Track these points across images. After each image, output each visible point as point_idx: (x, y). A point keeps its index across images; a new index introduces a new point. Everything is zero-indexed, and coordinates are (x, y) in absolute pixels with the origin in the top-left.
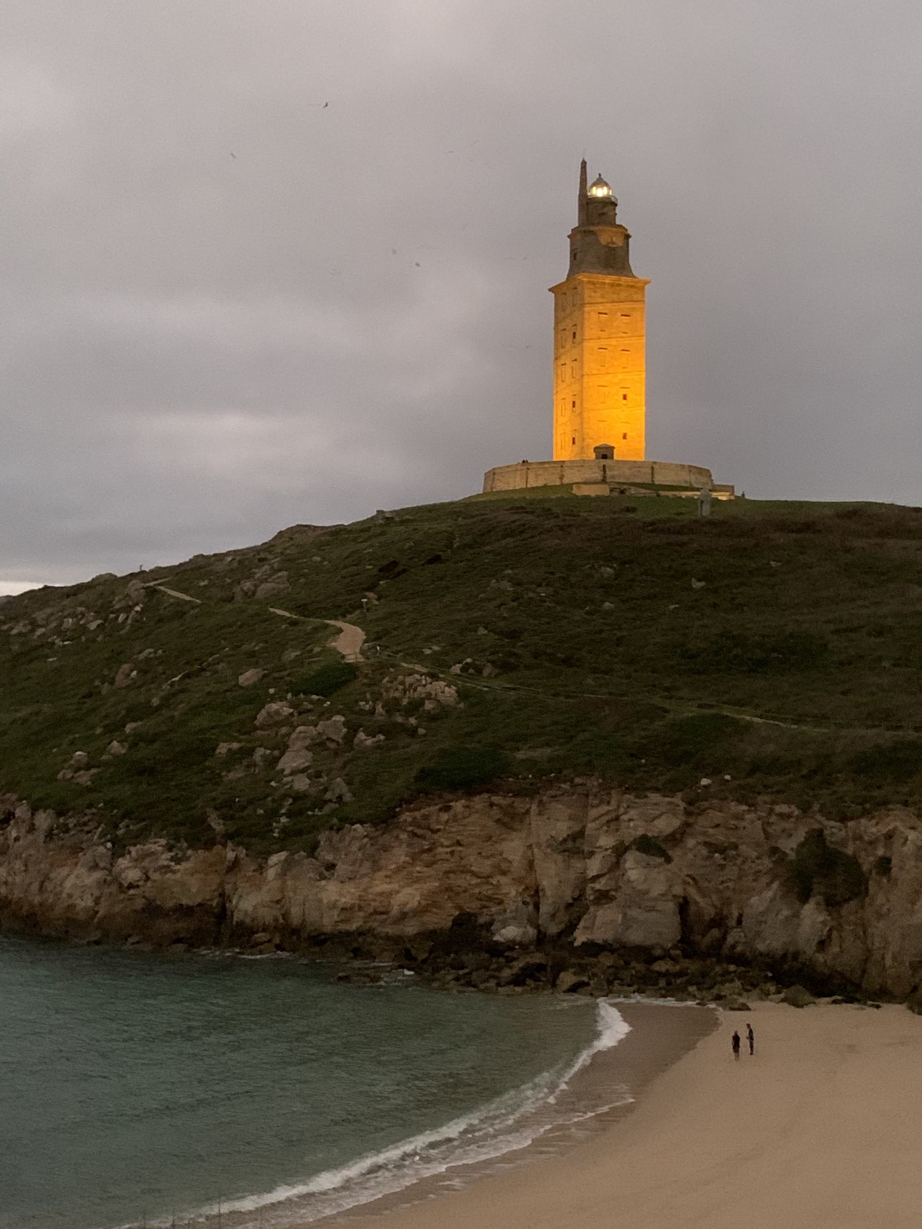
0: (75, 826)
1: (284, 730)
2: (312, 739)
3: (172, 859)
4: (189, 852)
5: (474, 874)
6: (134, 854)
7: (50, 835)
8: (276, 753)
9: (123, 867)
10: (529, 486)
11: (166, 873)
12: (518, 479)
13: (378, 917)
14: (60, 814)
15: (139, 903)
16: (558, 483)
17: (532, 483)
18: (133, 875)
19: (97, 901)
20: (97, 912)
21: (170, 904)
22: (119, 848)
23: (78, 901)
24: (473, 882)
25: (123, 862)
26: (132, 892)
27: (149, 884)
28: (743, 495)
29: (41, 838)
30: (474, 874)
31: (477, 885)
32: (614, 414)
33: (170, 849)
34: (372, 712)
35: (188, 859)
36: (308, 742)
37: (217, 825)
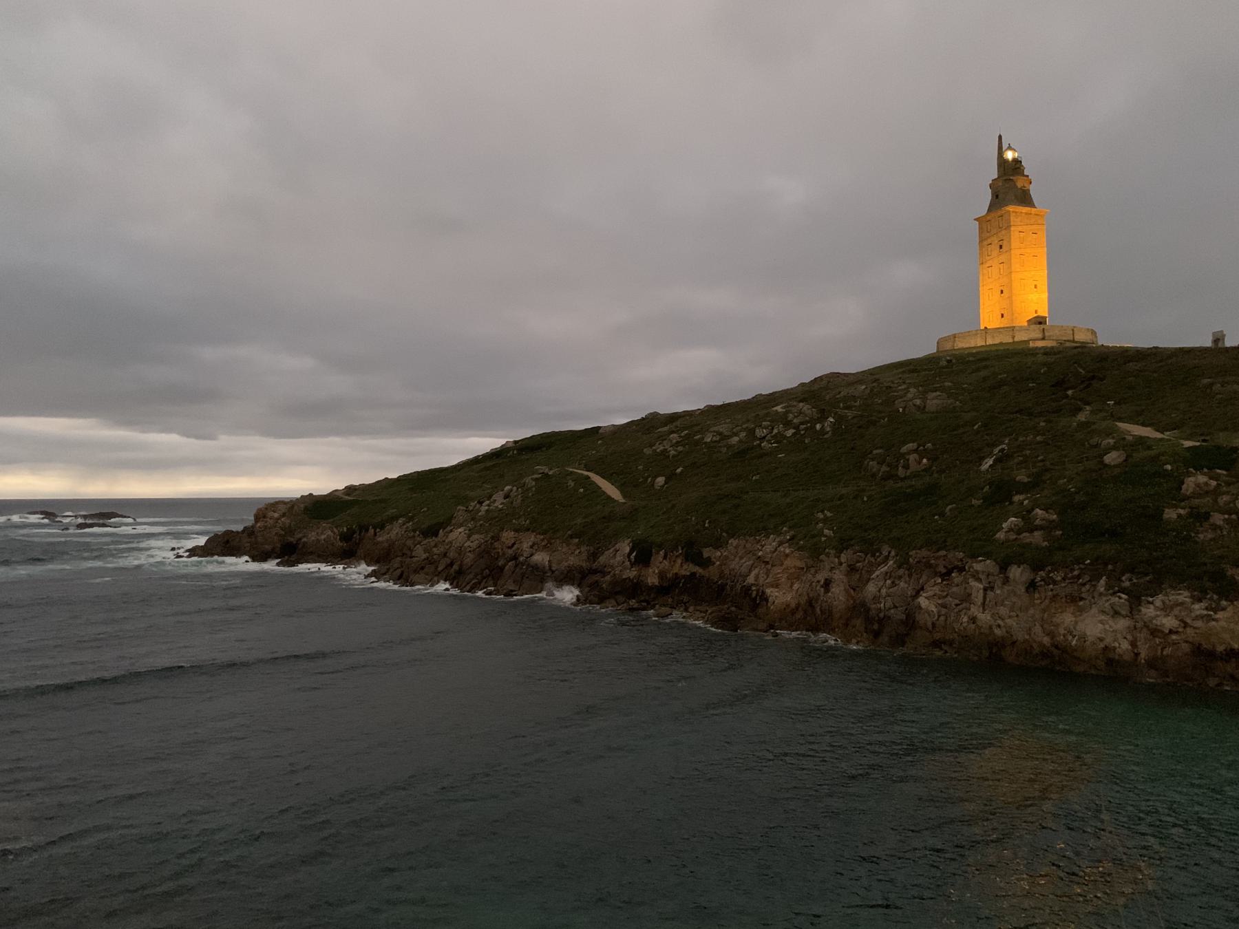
0: (1064, 579)
1: (1226, 498)
3: (1207, 609)
4: (1224, 603)
7: (1032, 586)
11: (1208, 622)
14: (1036, 568)
15: (1186, 647)
18: (1168, 622)
19: (1133, 644)
20: (1137, 655)
21: (1220, 648)
22: (1136, 599)
25: (1148, 611)
26: (1174, 637)
27: (1189, 630)
28: (1218, 339)
29: (1021, 589)
32: (1018, 296)
33: (1200, 600)
35: (1224, 609)
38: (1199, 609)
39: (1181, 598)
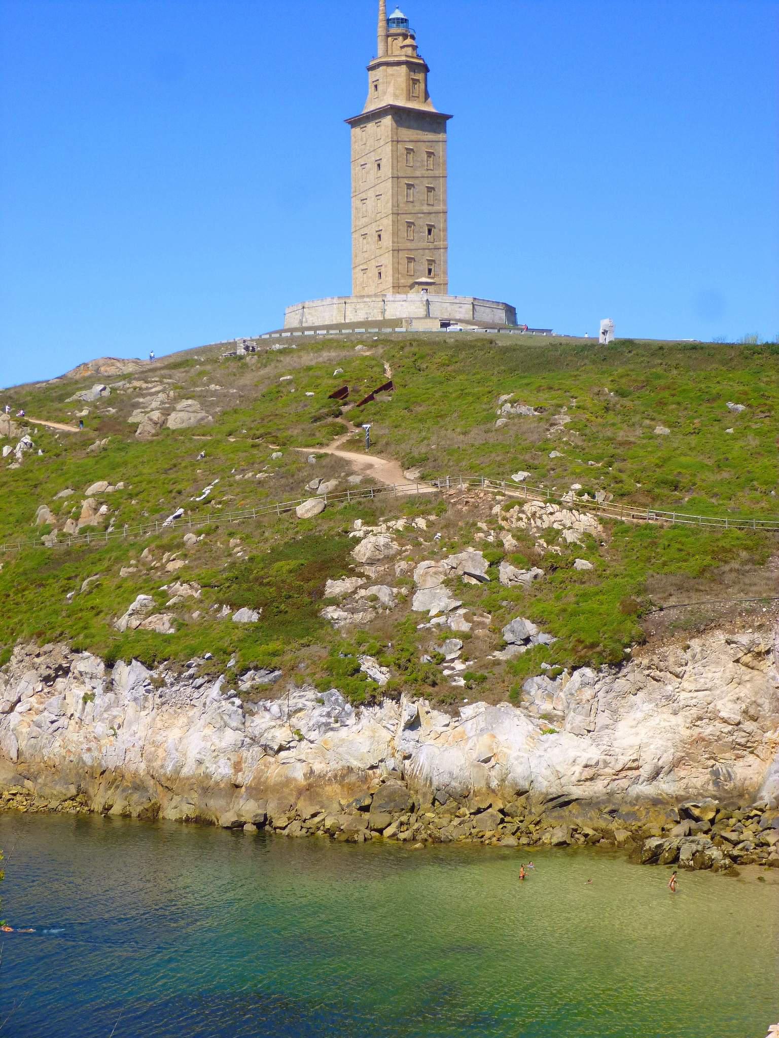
1: (403, 565)
2: (446, 575)
5: (725, 721)
6: (275, 709)
8: (404, 591)
9: (264, 726)
10: (347, 321)
12: (335, 312)
13: (630, 773)
16: (380, 318)
17: (351, 318)
19: (237, 767)
23: (212, 769)
24: (726, 730)
25: (261, 722)
30: (725, 721)
31: (730, 733)
34: (501, 544)
36: (442, 578)
37: (377, 673)
38: (318, 714)
39: (300, 703)
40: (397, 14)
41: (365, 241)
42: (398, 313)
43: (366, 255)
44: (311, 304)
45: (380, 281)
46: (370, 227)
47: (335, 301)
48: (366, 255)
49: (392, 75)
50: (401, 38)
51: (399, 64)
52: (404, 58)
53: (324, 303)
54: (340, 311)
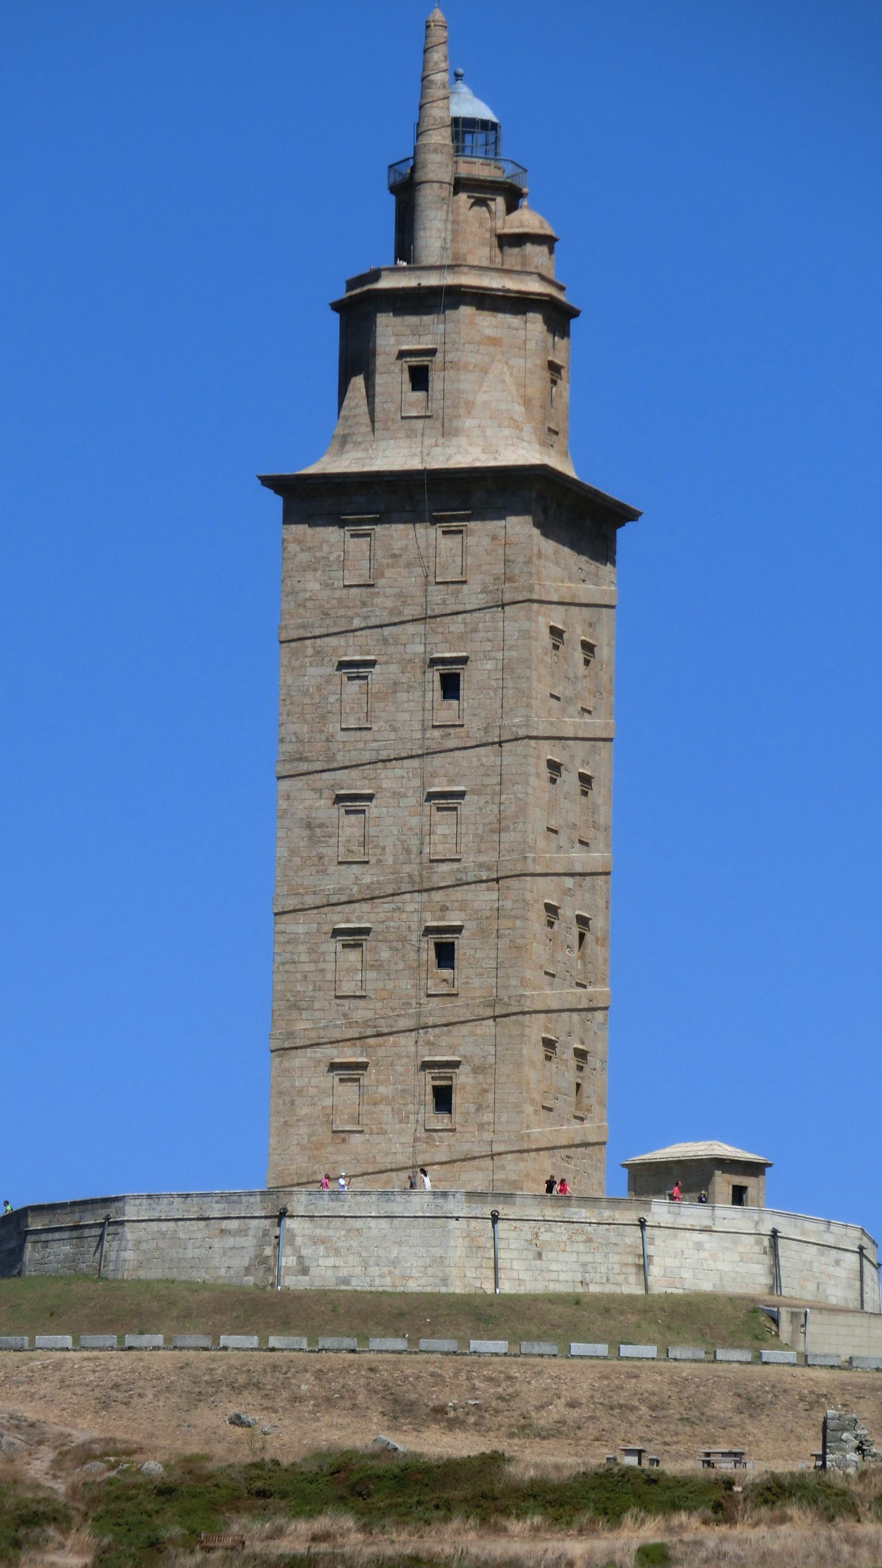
10: (506, 1287)
12: (457, 1249)
16: (632, 1288)
40: (470, 105)
41: (353, 956)
42: (687, 1274)
43: (361, 1012)
44: (325, 1205)
45: (442, 1121)
46: (385, 907)
47: (456, 1206)
48: (361, 1012)
49: (494, 341)
50: (499, 204)
51: (519, 304)
52: (534, 286)
53: (396, 1207)
54: (474, 1248)
